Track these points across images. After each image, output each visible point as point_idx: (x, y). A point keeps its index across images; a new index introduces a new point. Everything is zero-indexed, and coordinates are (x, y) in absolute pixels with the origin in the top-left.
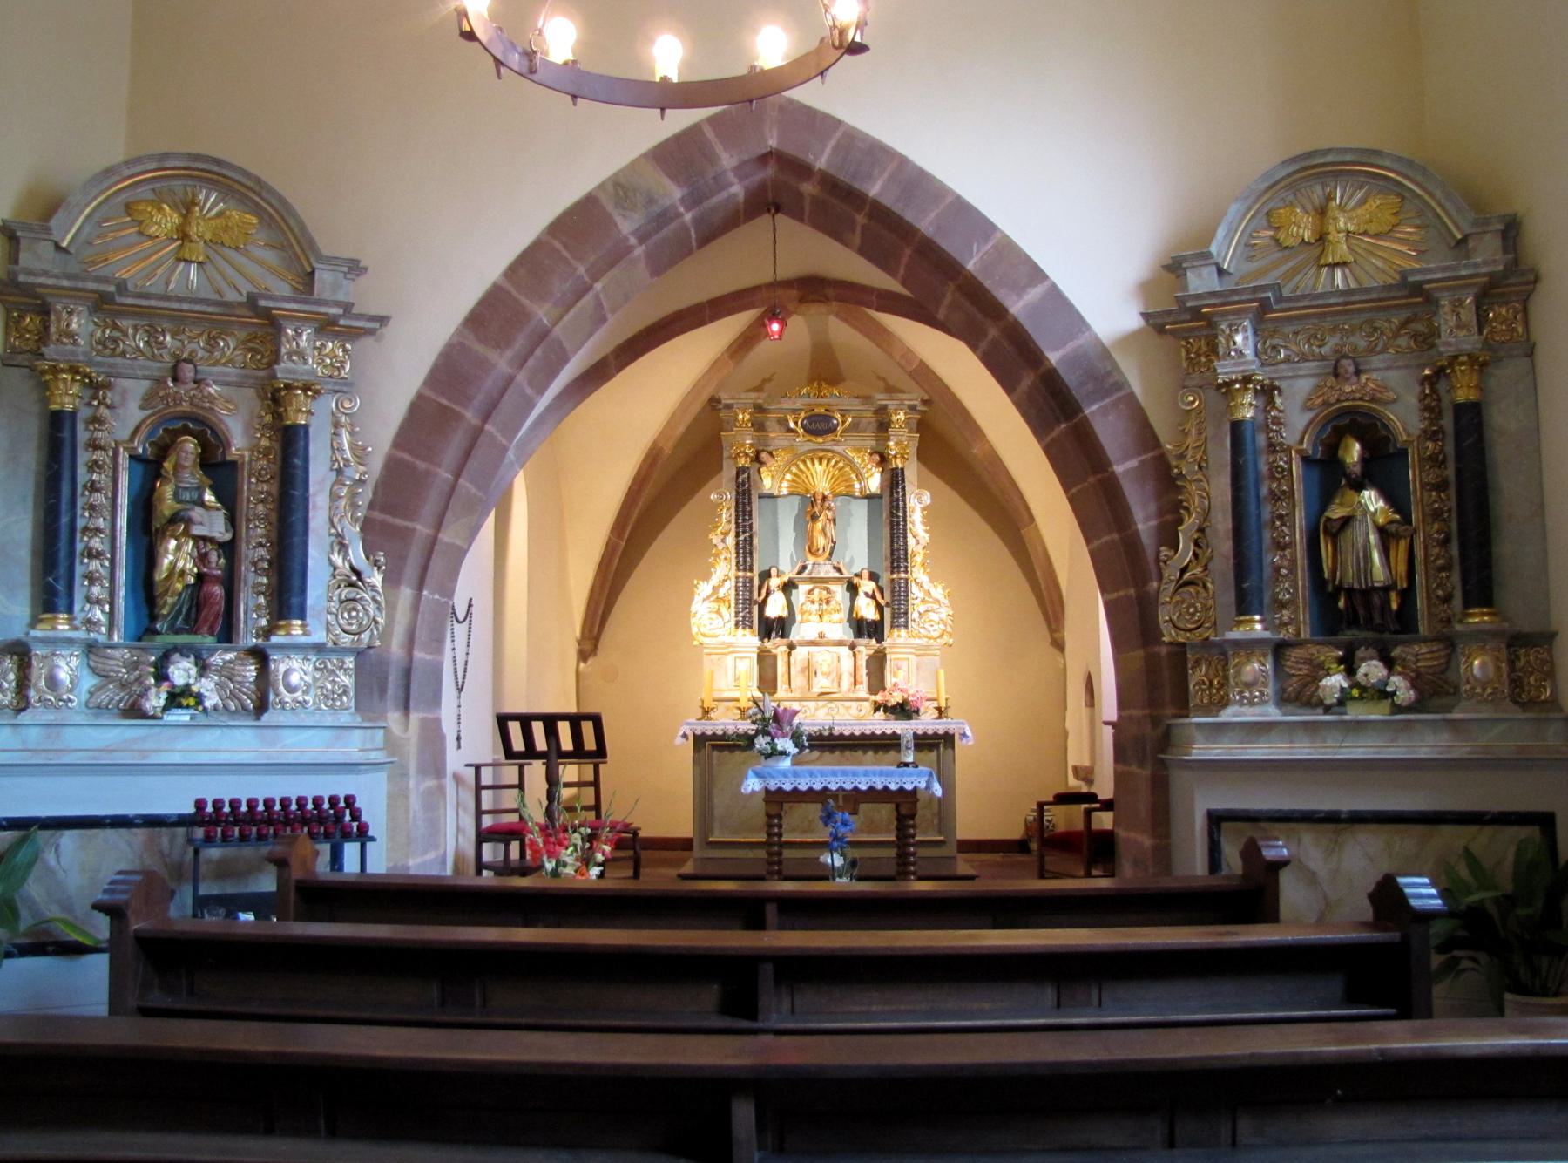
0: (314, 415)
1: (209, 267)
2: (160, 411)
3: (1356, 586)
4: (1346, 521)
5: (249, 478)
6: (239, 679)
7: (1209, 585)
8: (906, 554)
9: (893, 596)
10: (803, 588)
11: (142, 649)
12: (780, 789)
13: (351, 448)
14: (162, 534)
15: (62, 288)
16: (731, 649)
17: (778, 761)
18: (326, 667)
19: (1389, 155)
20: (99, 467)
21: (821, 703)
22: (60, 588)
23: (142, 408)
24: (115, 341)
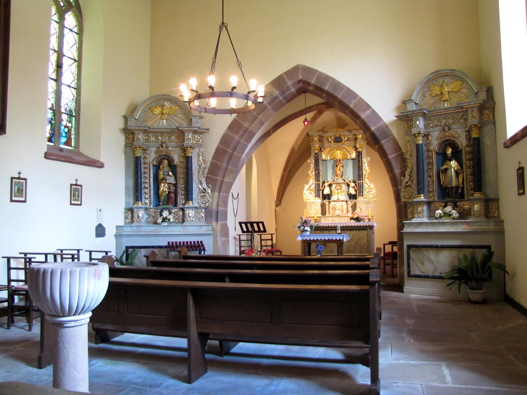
0: (194, 154)
1: (168, 120)
2: (159, 155)
3: (449, 186)
4: (446, 170)
5: (179, 169)
6: (178, 215)
7: (413, 187)
9: (359, 187)
10: (334, 186)
11: (157, 209)
12: (306, 240)
13: (202, 160)
14: (161, 183)
15: (137, 129)
16: (313, 203)
17: (306, 233)
18: (198, 212)
19: (457, 71)
20: (146, 168)
21: (338, 218)
22: (139, 196)
23: (155, 154)
24: (148, 139)
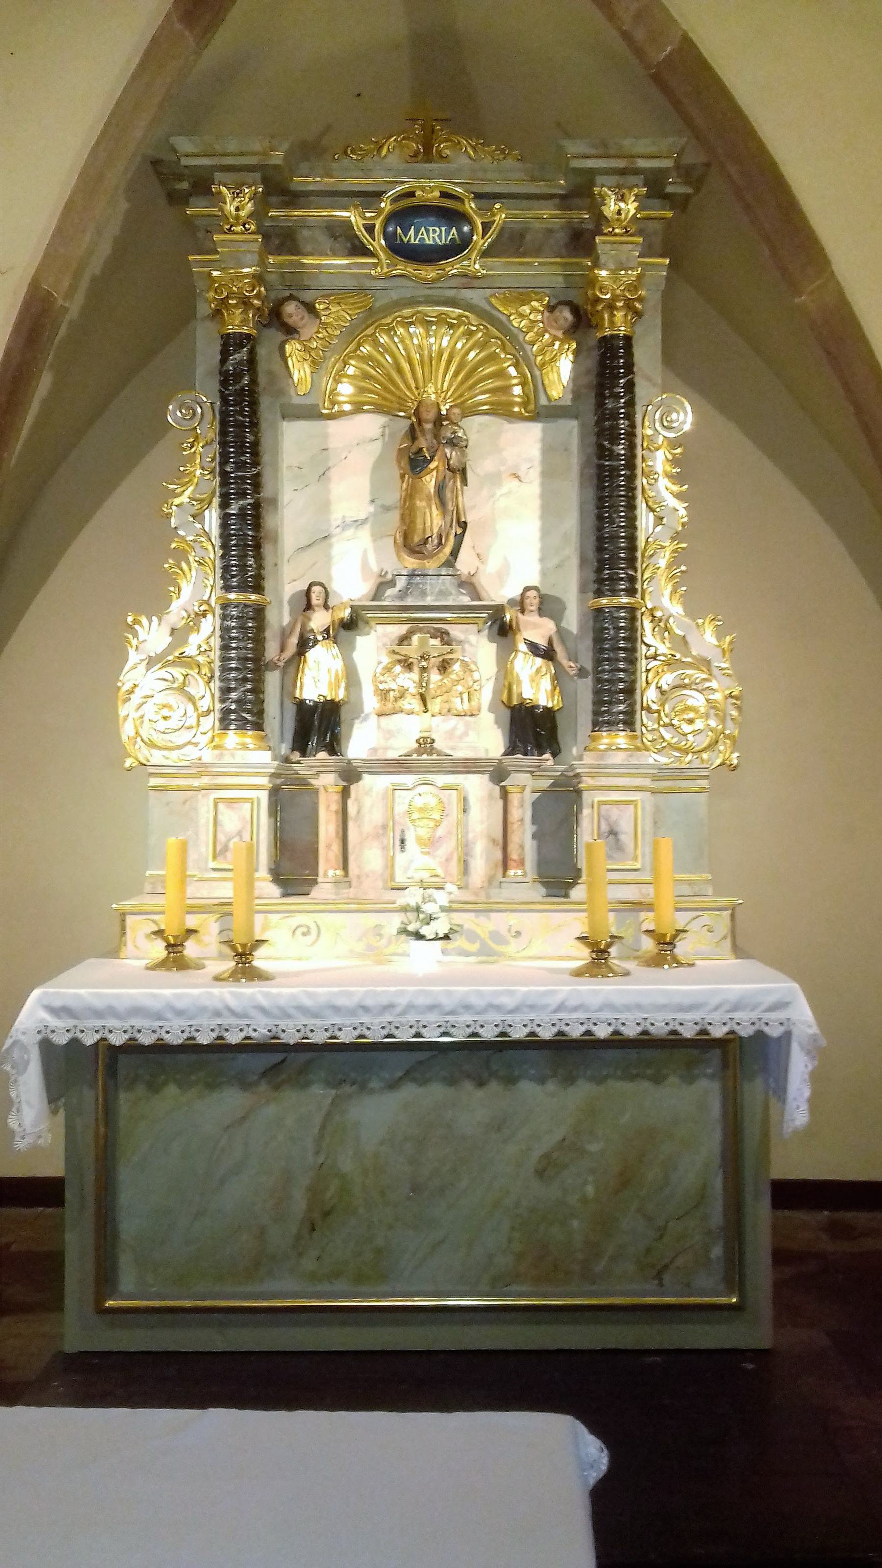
8: (632, 548)
